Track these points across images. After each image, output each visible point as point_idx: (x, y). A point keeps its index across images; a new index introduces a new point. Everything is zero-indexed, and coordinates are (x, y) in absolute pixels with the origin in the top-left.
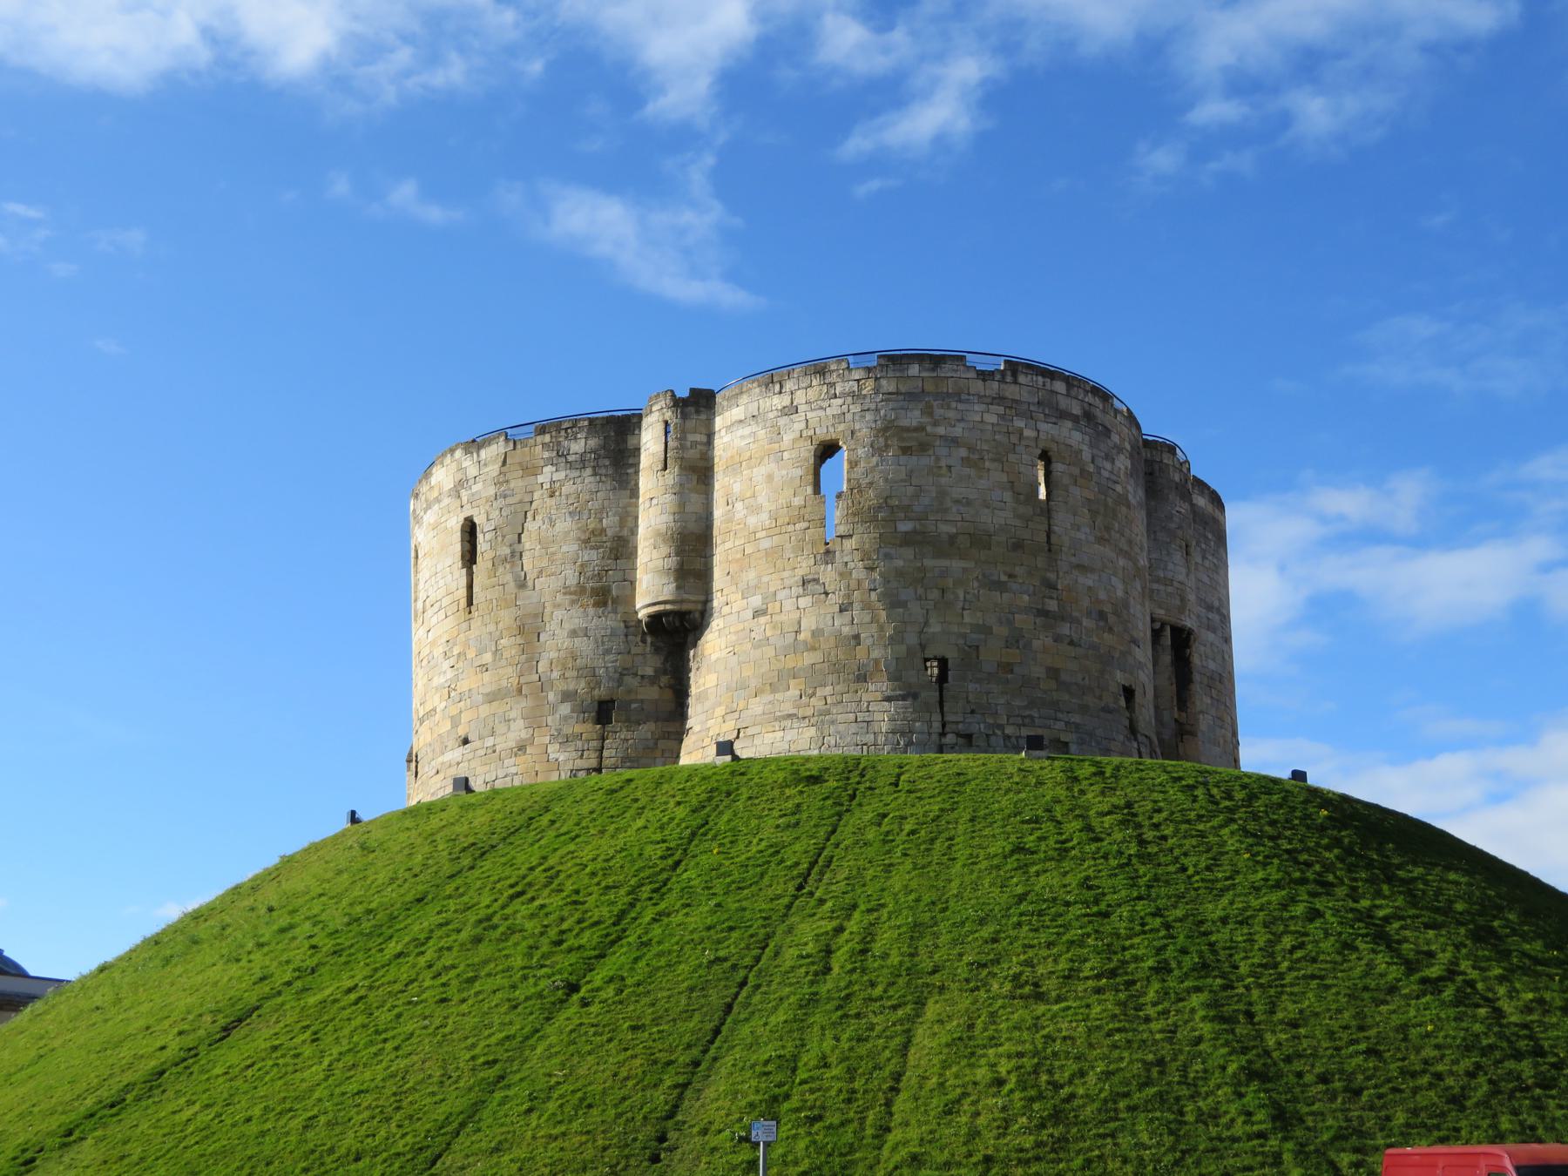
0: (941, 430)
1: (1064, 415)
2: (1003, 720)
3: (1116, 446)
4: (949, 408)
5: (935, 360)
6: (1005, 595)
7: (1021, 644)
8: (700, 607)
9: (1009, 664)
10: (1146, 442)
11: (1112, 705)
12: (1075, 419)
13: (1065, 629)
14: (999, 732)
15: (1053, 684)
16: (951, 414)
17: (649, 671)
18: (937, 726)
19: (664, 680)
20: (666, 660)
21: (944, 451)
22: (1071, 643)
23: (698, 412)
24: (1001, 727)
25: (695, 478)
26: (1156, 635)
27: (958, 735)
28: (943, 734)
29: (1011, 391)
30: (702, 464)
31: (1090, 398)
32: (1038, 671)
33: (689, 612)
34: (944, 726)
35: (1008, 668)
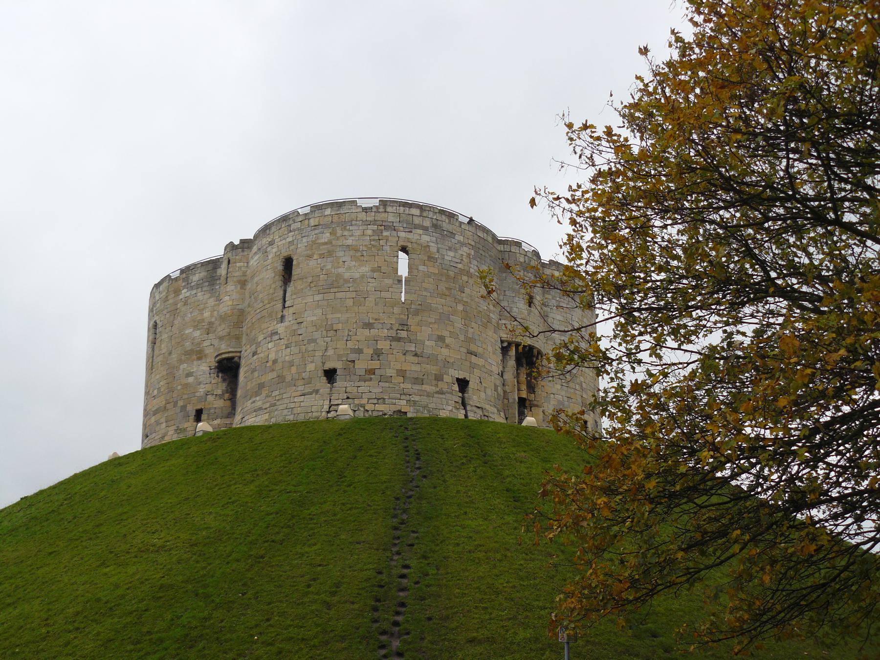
0: (340, 243)
1: (417, 227)
2: (364, 401)
3: (459, 242)
4: (345, 229)
5: (337, 205)
8: (238, 354)
9: (371, 369)
10: (500, 242)
11: (444, 390)
12: (425, 229)
14: (362, 409)
15: (401, 379)
16: (346, 233)
17: (219, 392)
18: (326, 408)
19: (227, 396)
20: (228, 385)
21: (341, 254)
22: (416, 355)
23: (243, 251)
24: (363, 406)
25: (239, 287)
26: (505, 350)
29: (381, 216)
30: (243, 279)
31: (438, 217)
33: (233, 358)
35: (372, 372)
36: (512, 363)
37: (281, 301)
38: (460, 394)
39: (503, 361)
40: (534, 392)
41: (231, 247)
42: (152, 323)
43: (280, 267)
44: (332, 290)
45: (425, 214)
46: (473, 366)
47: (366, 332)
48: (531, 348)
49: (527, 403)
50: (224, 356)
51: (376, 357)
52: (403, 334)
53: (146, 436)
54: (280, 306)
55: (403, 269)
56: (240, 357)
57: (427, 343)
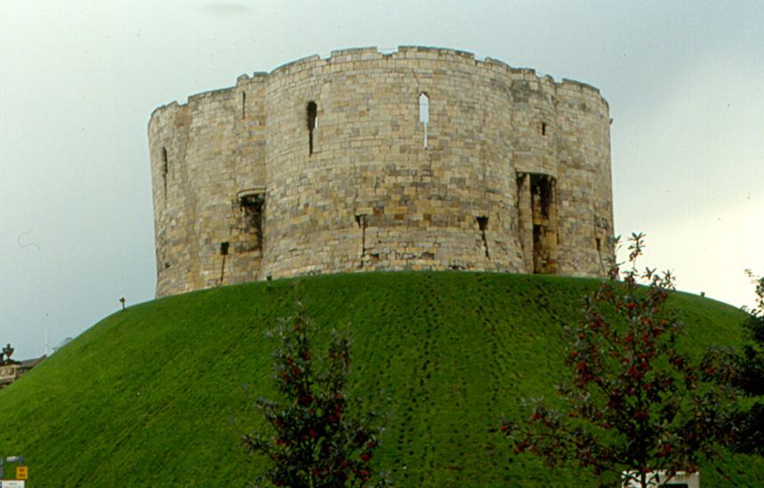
5: (359, 51)
6: (398, 178)
7: (408, 203)
8: (263, 191)
10: (514, 71)
13: (435, 192)
15: (428, 223)
17: (243, 225)
18: (360, 253)
22: (440, 198)
26: (520, 180)
27: (371, 255)
28: (363, 256)
30: (261, 114)
32: (419, 217)
34: (364, 250)
36: (528, 193)
37: (308, 146)
38: (481, 232)
39: (518, 192)
40: (548, 218)
41: (243, 79)
42: (159, 152)
43: (303, 108)
44: (359, 138)
45: (443, 58)
46: (492, 203)
47: (393, 179)
48: (545, 176)
49: (542, 230)
50: (248, 193)
51: (403, 203)
52: (427, 180)
53: (164, 266)
54: (308, 150)
55: (424, 117)
56: (264, 194)
57: (449, 187)
